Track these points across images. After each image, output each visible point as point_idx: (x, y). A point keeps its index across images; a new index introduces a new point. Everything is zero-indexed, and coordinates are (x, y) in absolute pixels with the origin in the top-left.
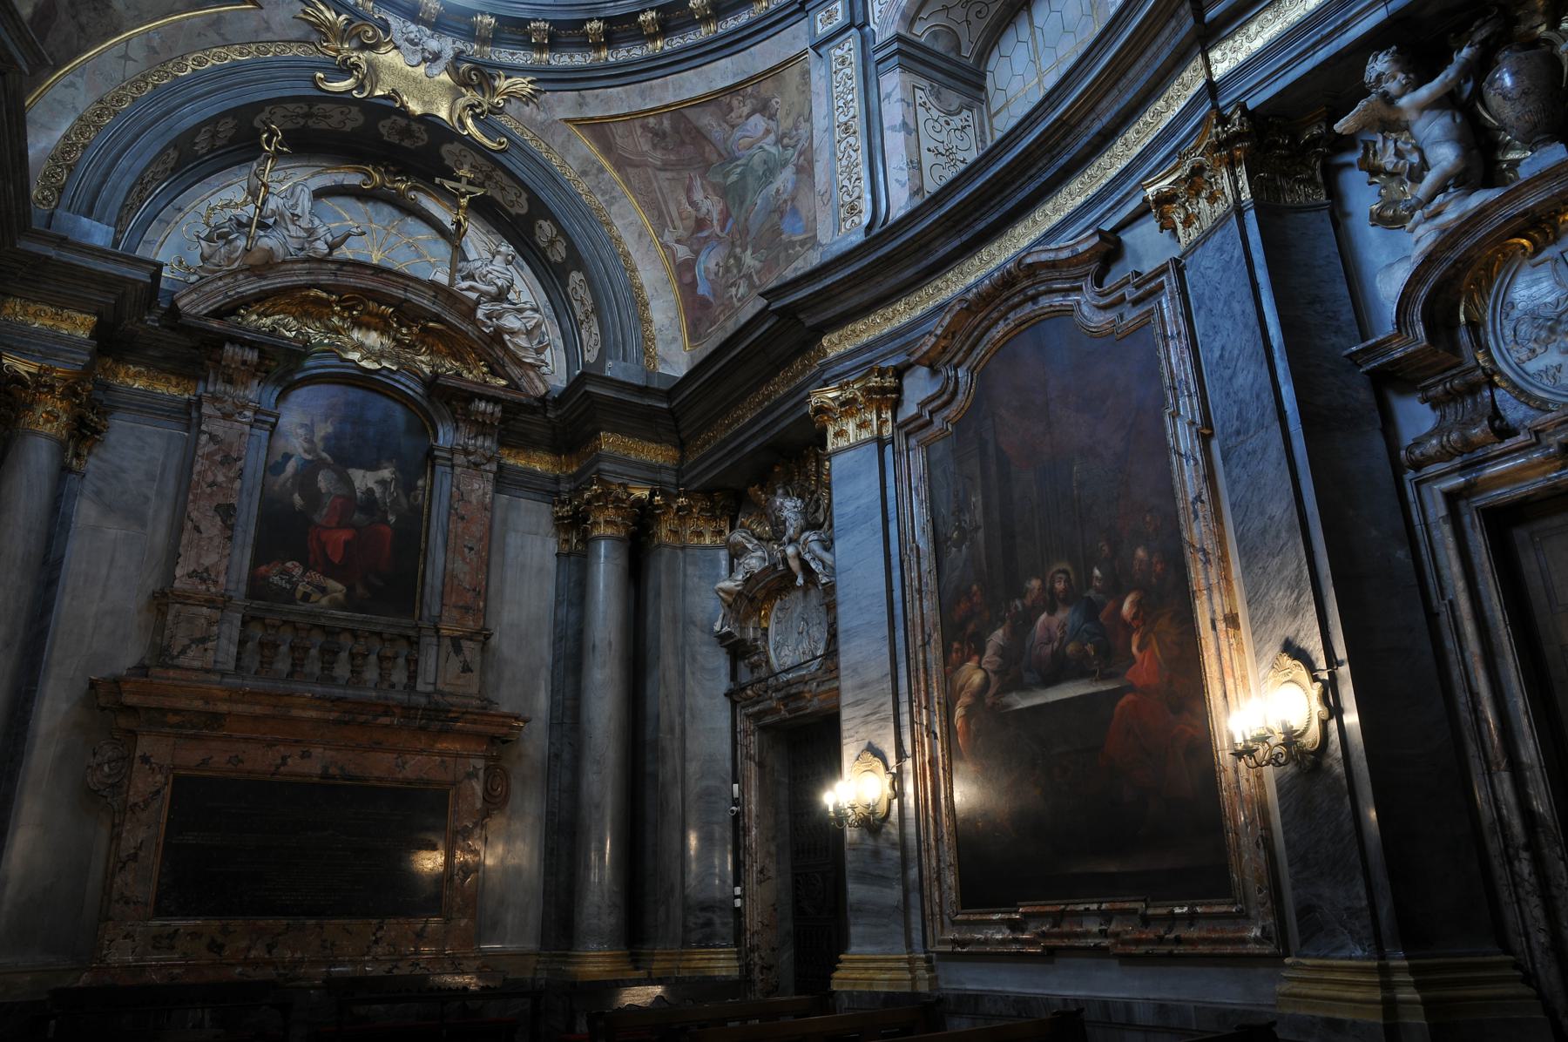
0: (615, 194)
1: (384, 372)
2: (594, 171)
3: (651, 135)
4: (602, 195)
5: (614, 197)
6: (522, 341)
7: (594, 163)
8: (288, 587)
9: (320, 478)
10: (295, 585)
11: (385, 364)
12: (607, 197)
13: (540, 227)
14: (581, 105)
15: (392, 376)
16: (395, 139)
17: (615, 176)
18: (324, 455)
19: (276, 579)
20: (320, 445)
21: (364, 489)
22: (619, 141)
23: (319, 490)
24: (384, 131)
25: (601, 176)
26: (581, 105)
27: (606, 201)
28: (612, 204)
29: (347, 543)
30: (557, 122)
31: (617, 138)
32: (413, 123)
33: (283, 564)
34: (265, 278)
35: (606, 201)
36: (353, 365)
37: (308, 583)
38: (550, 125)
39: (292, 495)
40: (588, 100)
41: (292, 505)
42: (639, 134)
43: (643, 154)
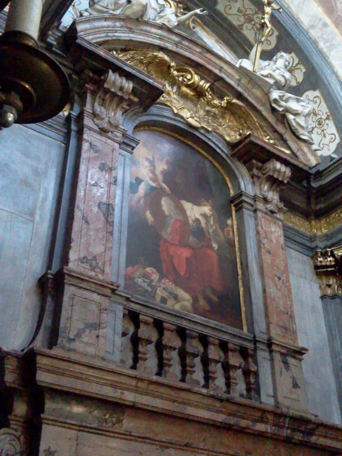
0: (334, 42)
1: (202, 131)
2: (320, 25)
4: (325, 43)
5: (333, 45)
6: (301, 121)
7: (320, 19)
8: (150, 289)
9: (163, 202)
10: (154, 288)
11: (203, 125)
15: (207, 135)
17: (336, 30)
18: (164, 186)
19: (140, 281)
20: (160, 177)
21: (193, 218)
23: (163, 212)
25: (324, 29)
27: (327, 47)
28: (331, 50)
29: (188, 259)
33: (144, 268)
34: (133, 32)
35: (327, 47)
36: (182, 120)
37: (164, 289)
39: (145, 212)
41: (146, 220)
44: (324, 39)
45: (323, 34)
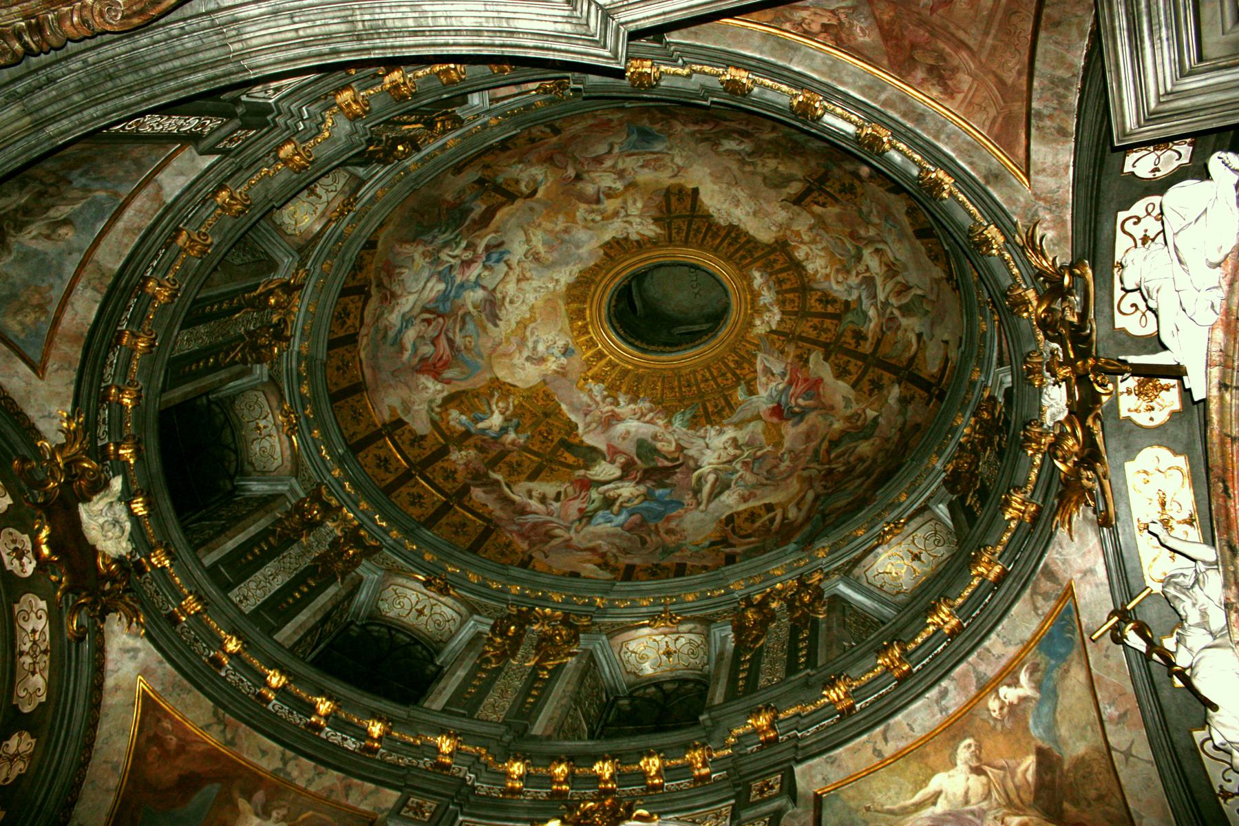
24: (1161, 417)
26: (996, 176)
38: (1045, 200)
40: (984, 172)
43: (975, 77)
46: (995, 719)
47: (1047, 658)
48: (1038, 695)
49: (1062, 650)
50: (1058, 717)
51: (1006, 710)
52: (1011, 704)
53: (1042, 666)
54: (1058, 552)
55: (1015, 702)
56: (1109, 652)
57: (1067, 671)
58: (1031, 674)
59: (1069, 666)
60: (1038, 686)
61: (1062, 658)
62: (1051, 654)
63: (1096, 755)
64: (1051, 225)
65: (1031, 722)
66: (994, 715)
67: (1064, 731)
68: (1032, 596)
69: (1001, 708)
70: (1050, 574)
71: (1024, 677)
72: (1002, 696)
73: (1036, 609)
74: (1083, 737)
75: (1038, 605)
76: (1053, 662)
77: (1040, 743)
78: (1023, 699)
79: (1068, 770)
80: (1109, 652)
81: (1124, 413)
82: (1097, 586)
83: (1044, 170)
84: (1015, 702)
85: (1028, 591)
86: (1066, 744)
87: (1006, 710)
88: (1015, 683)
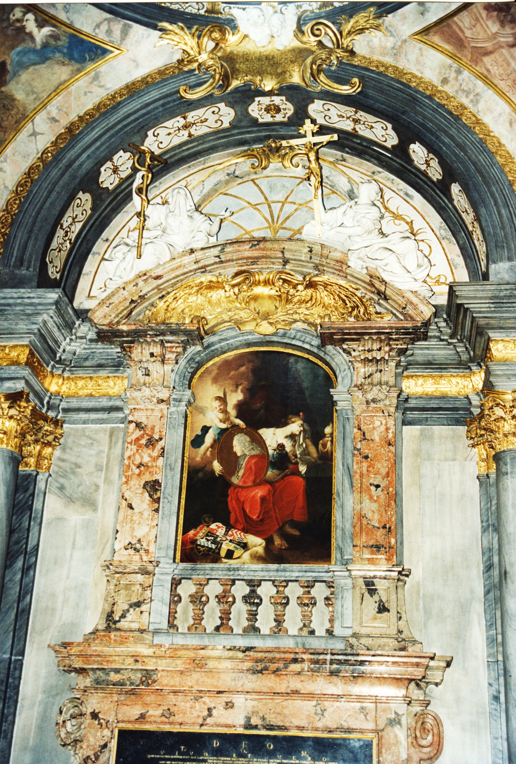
3: (495, 13)
4: (467, 96)
8: (214, 547)
9: (235, 442)
10: (219, 544)
12: (471, 97)
13: (414, 152)
14: (422, 14)
16: (267, 118)
18: (238, 421)
19: (203, 542)
20: (233, 413)
21: (275, 446)
22: (468, 33)
23: (235, 453)
25: (460, 77)
26: (422, 14)
27: (472, 101)
28: (477, 101)
29: (263, 499)
30: (405, 41)
31: (465, 30)
32: (274, 98)
33: (208, 526)
37: (231, 541)
38: (401, 47)
39: (212, 462)
41: (213, 472)
42: (485, 18)
44: (464, 91)
45: (461, 85)
46: (8, 19)
47: (67, 45)
48: (39, 47)
49: (76, 56)
50: (31, 69)
51: (18, 25)
52: (24, 28)
53: (60, 43)
54: (143, 34)
55: (27, 30)
56: (88, 94)
57: (63, 64)
58: (51, 36)
59: (68, 65)
60: (45, 45)
61: (71, 58)
62: (70, 47)
63: (21, 109)
64: (383, 44)
65: (19, 49)
66: (11, 16)
67: (25, 76)
68: (106, 19)
69: (18, 20)
70: (125, 32)
71: (47, 30)
72: (26, 18)
73: (98, 26)
74: (28, 95)
75: (102, 27)
76: (65, 51)
77: (8, 62)
78: (31, 36)
79: (2, 92)
80: (88, 94)
81: (257, 99)
82: (129, 72)
83: (422, 55)
84: (27, 30)
85: (109, 16)
86: (17, 83)
87: (18, 25)
88: (40, 25)
